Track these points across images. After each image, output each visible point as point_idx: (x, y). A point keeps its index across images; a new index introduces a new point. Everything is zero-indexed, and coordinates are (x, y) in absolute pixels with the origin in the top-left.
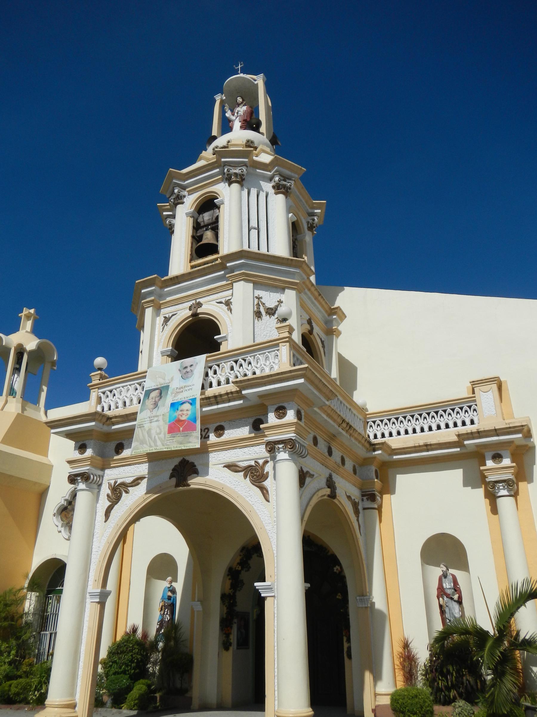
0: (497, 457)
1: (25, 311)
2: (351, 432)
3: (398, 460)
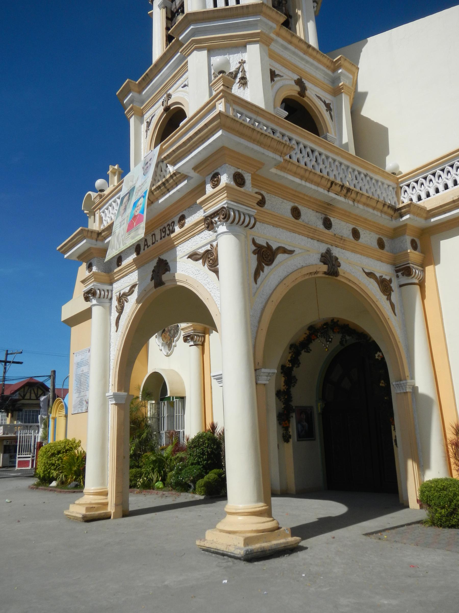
1: (111, 168)
2: (353, 195)
3: (441, 222)
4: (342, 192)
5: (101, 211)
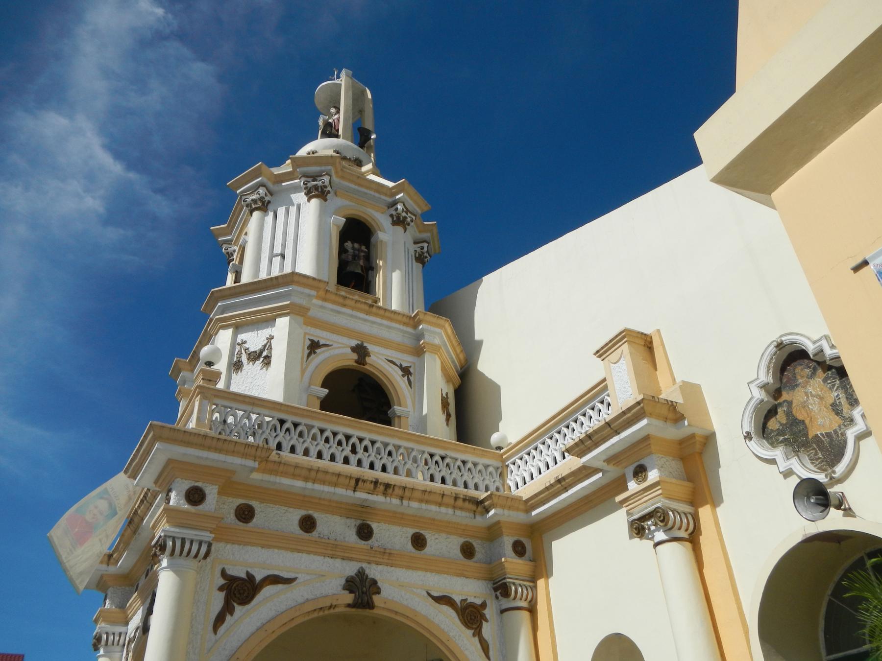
0: (640, 471)
2: (398, 491)
4: (377, 489)
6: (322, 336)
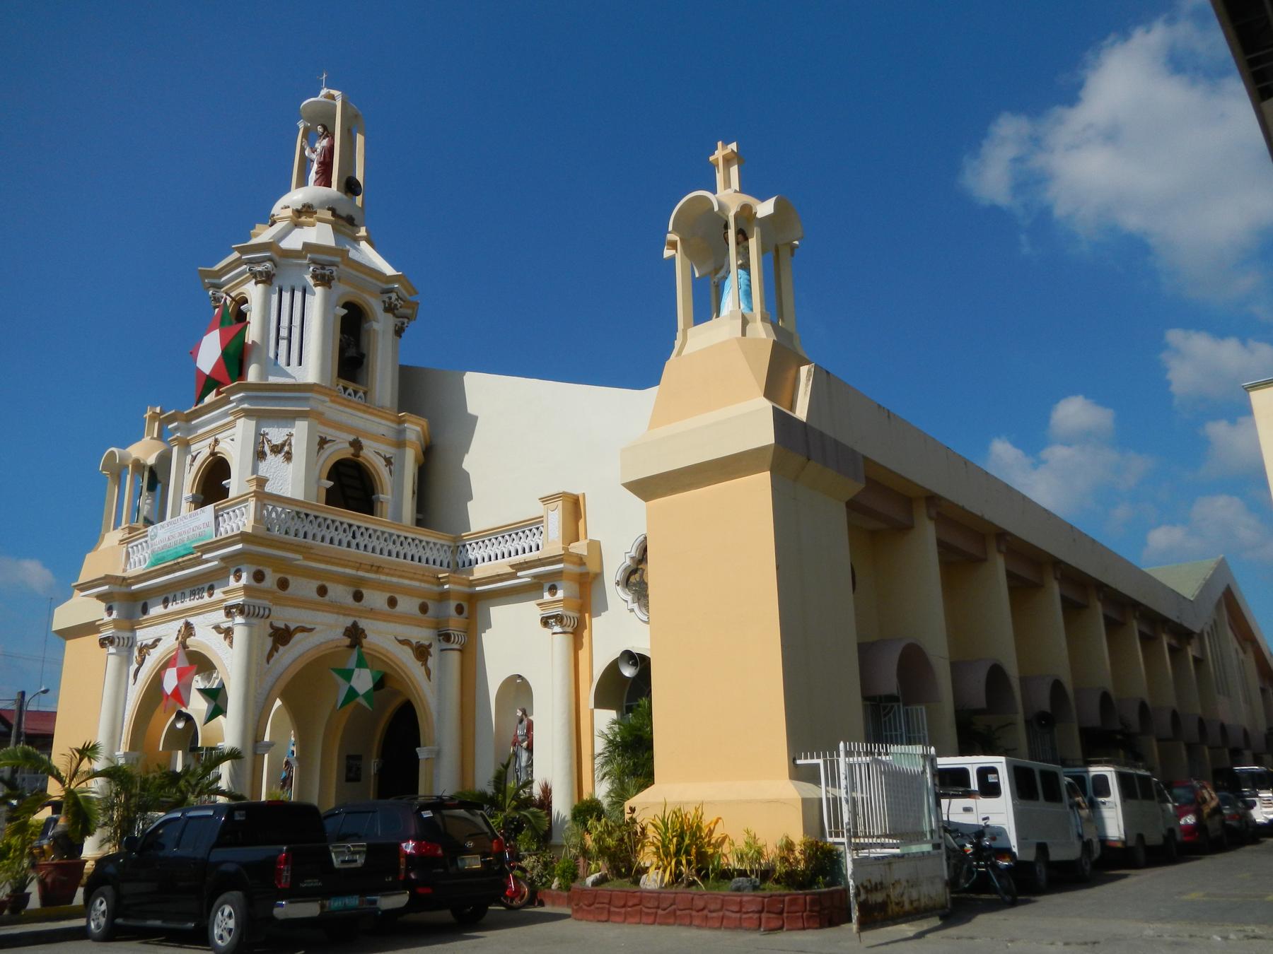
0: (553, 589)
5: (130, 545)
6: (329, 433)
